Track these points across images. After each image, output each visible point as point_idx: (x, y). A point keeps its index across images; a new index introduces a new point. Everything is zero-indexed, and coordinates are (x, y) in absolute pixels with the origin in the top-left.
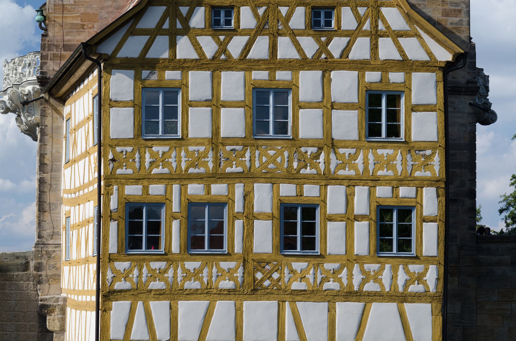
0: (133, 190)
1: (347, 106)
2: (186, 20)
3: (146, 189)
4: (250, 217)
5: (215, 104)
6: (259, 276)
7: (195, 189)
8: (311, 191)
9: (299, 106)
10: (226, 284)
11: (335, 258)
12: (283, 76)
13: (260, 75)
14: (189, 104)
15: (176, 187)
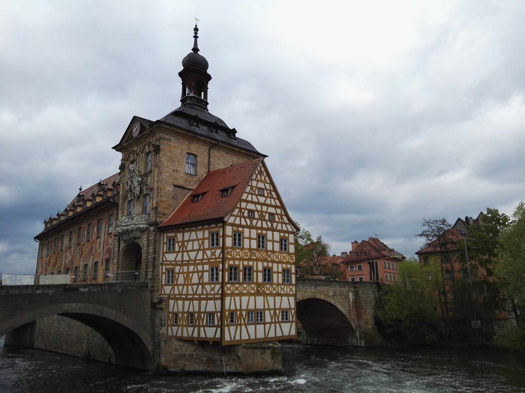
0: (231, 262)
1: (277, 242)
2: (243, 214)
3: (234, 262)
4: (257, 271)
5: (250, 238)
6: (259, 289)
7: (246, 263)
8: (270, 265)
9: (267, 241)
10: (252, 291)
11: (275, 284)
12: (264, 232)
13: (259, 231)
14: (244, 238)
15: (241, 262)
